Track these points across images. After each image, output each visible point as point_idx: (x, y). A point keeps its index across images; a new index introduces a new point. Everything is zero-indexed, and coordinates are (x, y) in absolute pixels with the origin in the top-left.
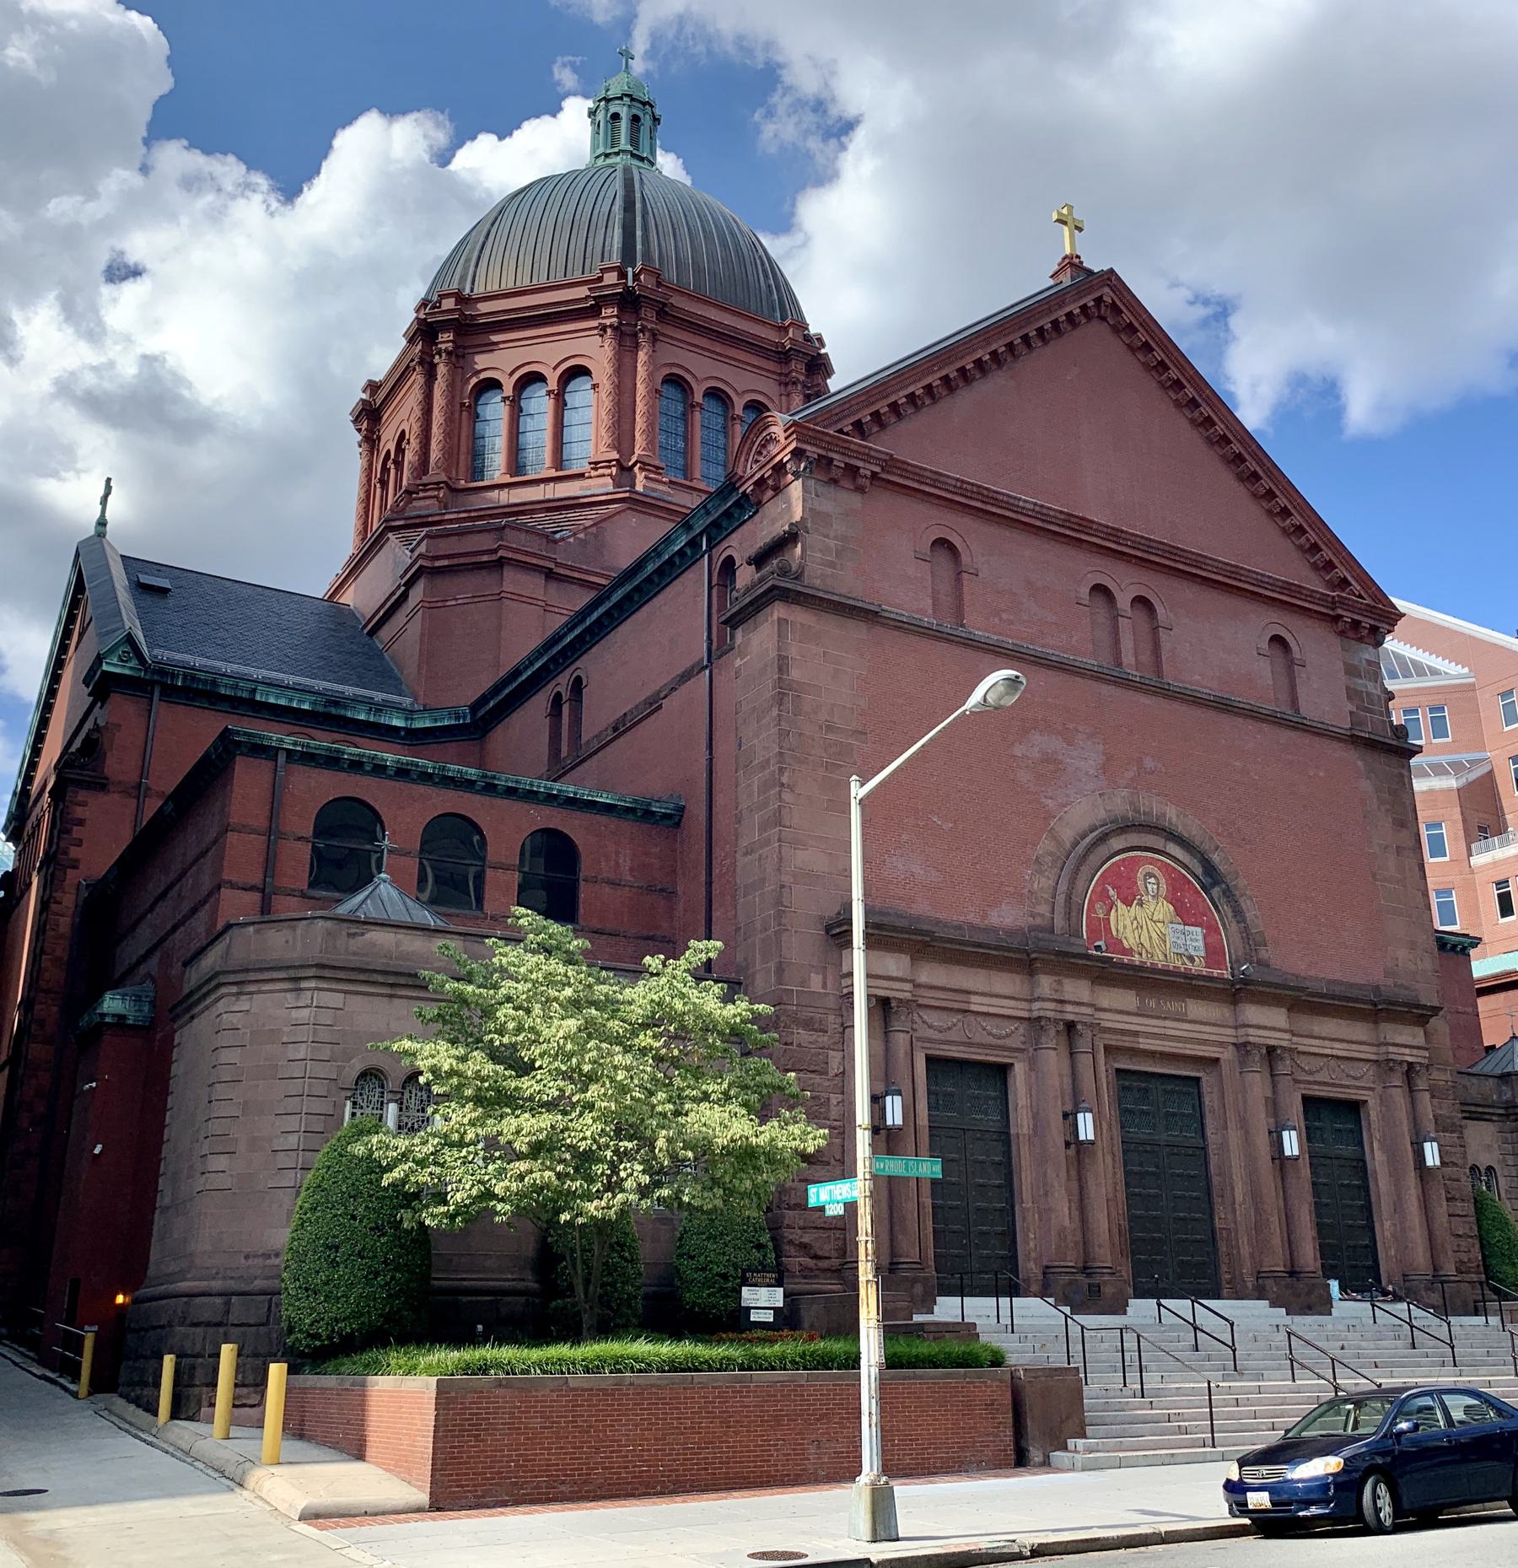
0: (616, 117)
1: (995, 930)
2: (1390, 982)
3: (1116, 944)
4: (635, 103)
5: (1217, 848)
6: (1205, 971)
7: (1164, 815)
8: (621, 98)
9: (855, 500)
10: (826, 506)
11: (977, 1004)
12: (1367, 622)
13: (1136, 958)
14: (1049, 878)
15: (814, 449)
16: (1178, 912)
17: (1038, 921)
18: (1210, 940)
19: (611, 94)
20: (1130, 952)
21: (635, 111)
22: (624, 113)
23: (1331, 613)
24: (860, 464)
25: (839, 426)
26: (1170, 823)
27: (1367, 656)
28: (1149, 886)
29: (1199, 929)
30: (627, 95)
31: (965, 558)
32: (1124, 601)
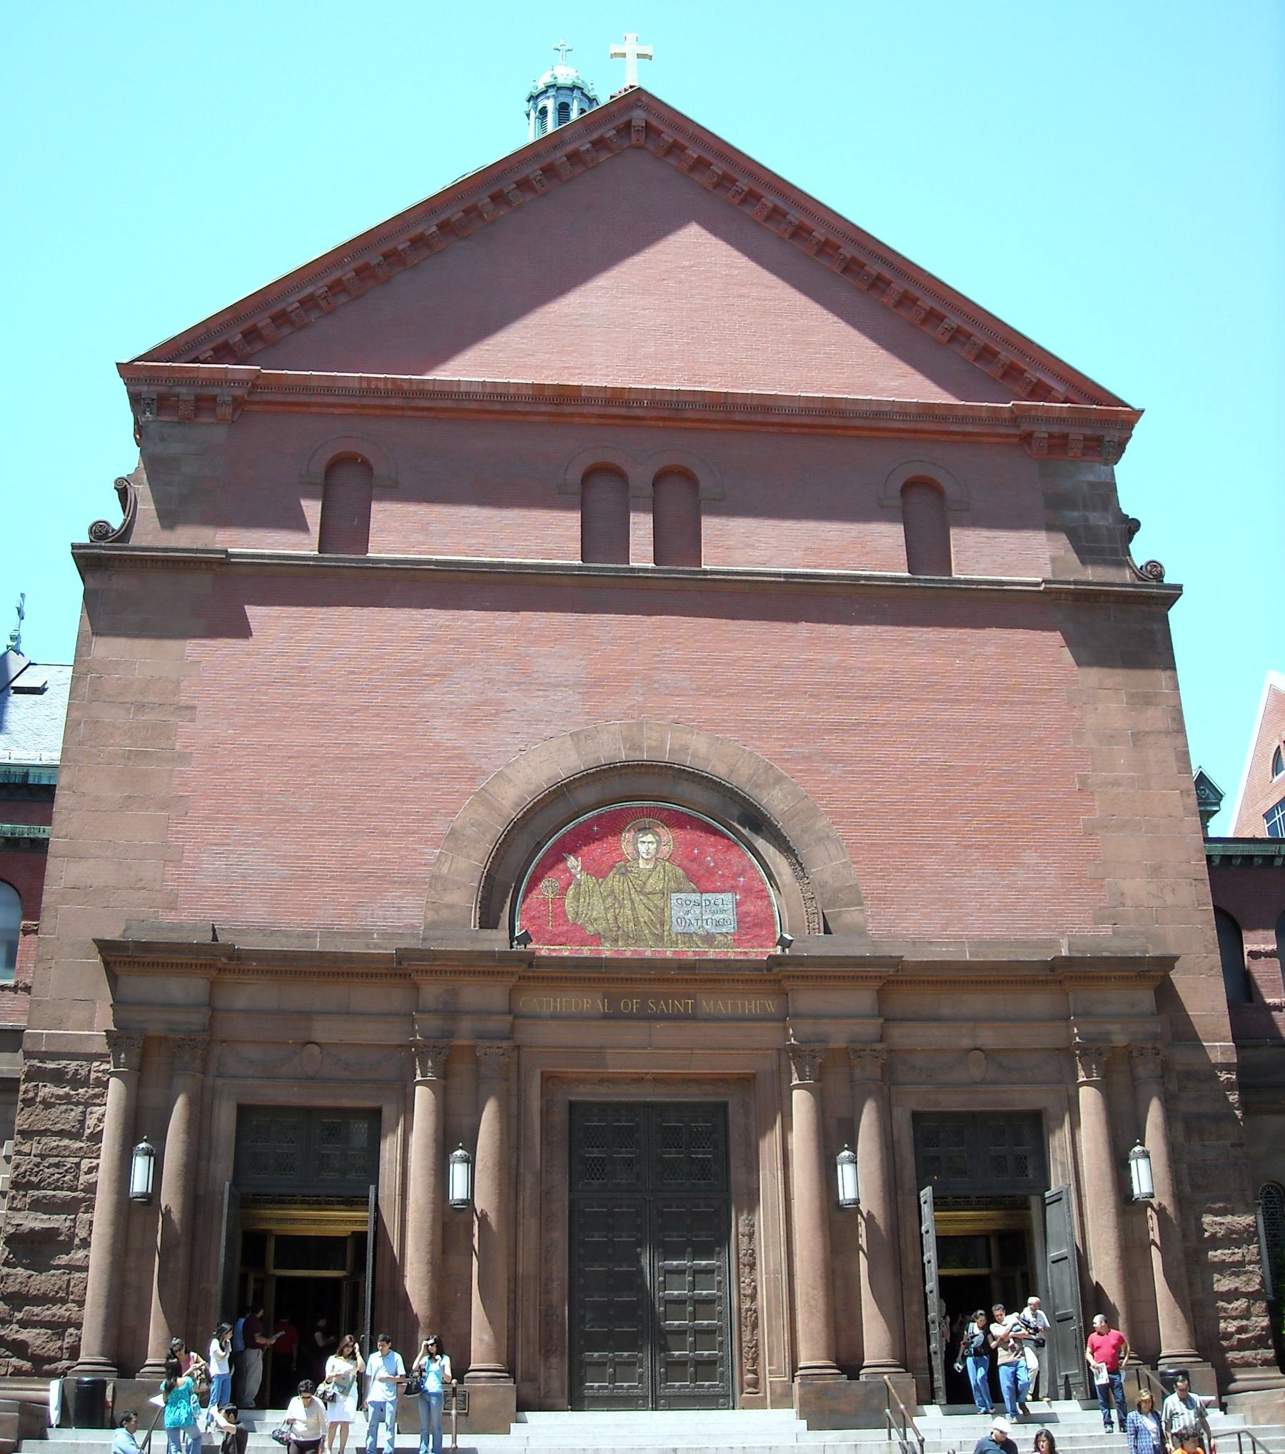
0: (543, 112)
1: (367, 934)
2: (1106, 930)
3: (576, 934)
4: (561, 92)
5: (779, 779)
6: (732, 954)
7: (685, 748)
8: (546, 92)
9: (219, 434)
10: (174, 448)
11: (323, 1031)
12: (1076, 433)
13: (607, 951)
14: (469, 857)
15: (153, 388)
16: (690, 876)
17: (445, 914)
18: (749, 907)
19: (536, 92)
20: (597, 938)
21: (562, 99)
22: (550, 104)
23: (1012, 431)
24: (216, 391)
25: (192, 356)
26: (695, 756)
27: (1091, 478)
28: (642, 848)
29: (728, 897)
30: (549, 87)
31: (379, 468)
32: (641, 476)
